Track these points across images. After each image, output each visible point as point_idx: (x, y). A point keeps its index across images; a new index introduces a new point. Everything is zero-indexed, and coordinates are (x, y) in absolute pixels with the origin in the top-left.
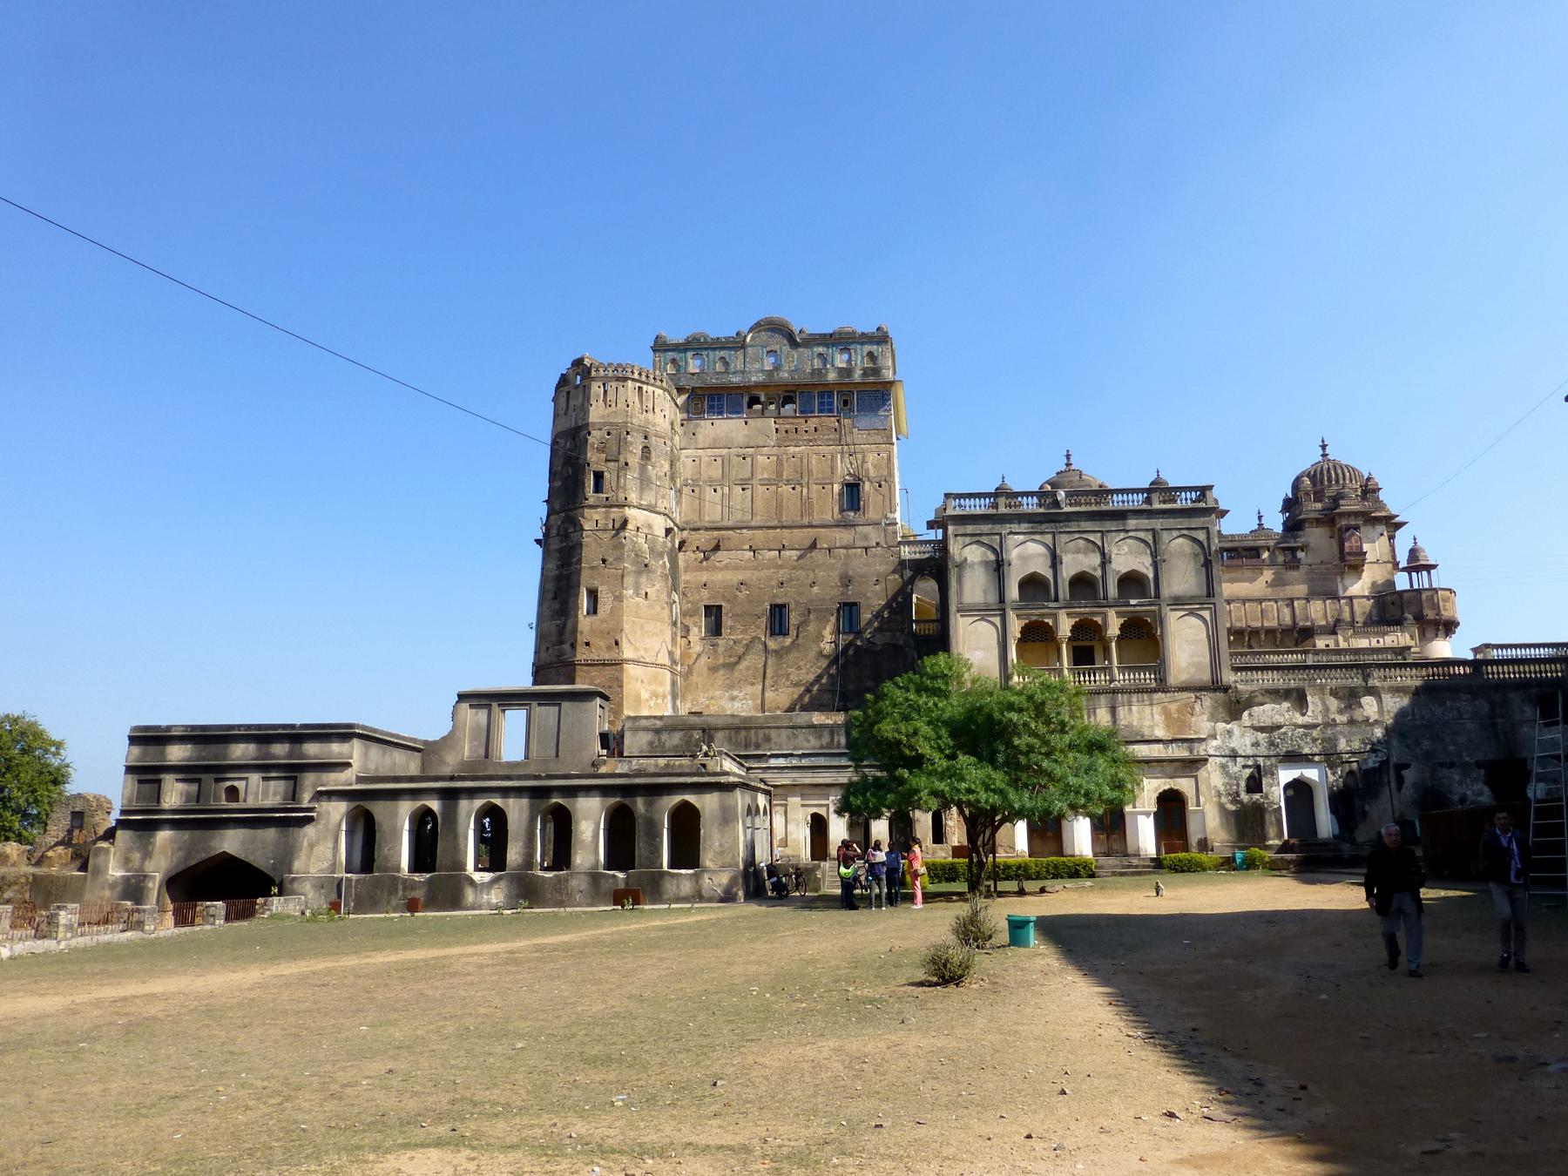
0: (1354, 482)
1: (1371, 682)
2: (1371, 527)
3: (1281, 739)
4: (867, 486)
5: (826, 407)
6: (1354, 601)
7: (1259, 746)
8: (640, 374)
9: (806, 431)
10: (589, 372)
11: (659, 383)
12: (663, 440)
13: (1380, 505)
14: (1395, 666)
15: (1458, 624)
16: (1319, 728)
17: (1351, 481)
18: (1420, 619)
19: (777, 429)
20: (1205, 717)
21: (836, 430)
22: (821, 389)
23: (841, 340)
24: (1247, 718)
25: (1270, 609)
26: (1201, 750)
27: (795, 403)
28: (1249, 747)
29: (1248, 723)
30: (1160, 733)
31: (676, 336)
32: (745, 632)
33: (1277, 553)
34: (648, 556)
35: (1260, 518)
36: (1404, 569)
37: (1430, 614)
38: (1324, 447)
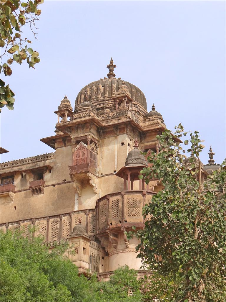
2: (114, 138)
6: (73, 215)
33: (28, 177)
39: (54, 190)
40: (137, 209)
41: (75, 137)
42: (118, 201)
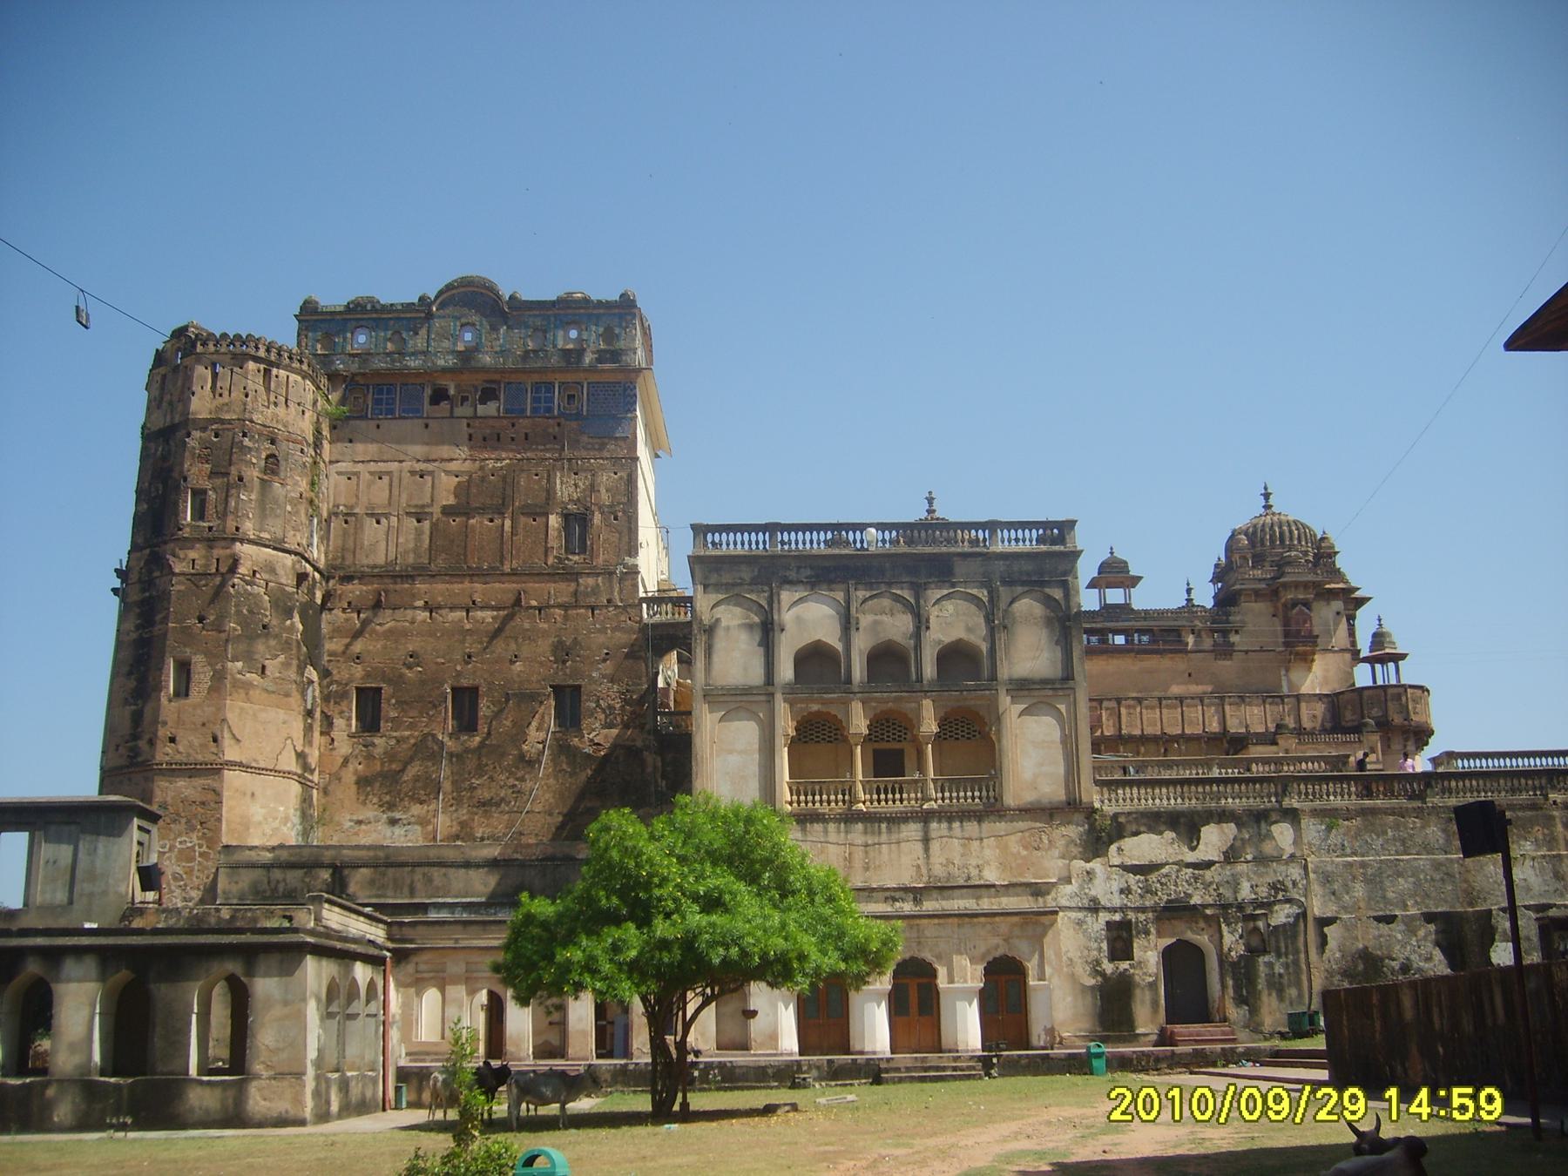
0: (1303, 543)
1: (1286, 803)
3: (1162, 884)
4: (597, 518)
5: (543, 405)
7: (1130, 893)
8: (268, 351)
9: (513, 439)
10: (194, 346)
11: (296, 365)
12: (299, 446)
13: (1337, 574)
14: (1327, 779)
15: (1432, 733)
16: (1213, 868)
17: (1299, 541)
18: (1384, 726)
19: (470, 435)
20: (1056, 853)
21: (555, 438)
22: (536, 378)
23: (569, 310)
24: (1115, 855)
26: (1050, 902)
27: (497, 398)
28: (1116, 895)
29: (1116, 861)
30: (992, 876)
31: (333, 298)
32: (412, 726)
34: (268, 613)
35: (1189, 591)
36: (1365, 660)
37: (1397, 720)
38: (1267, 496)
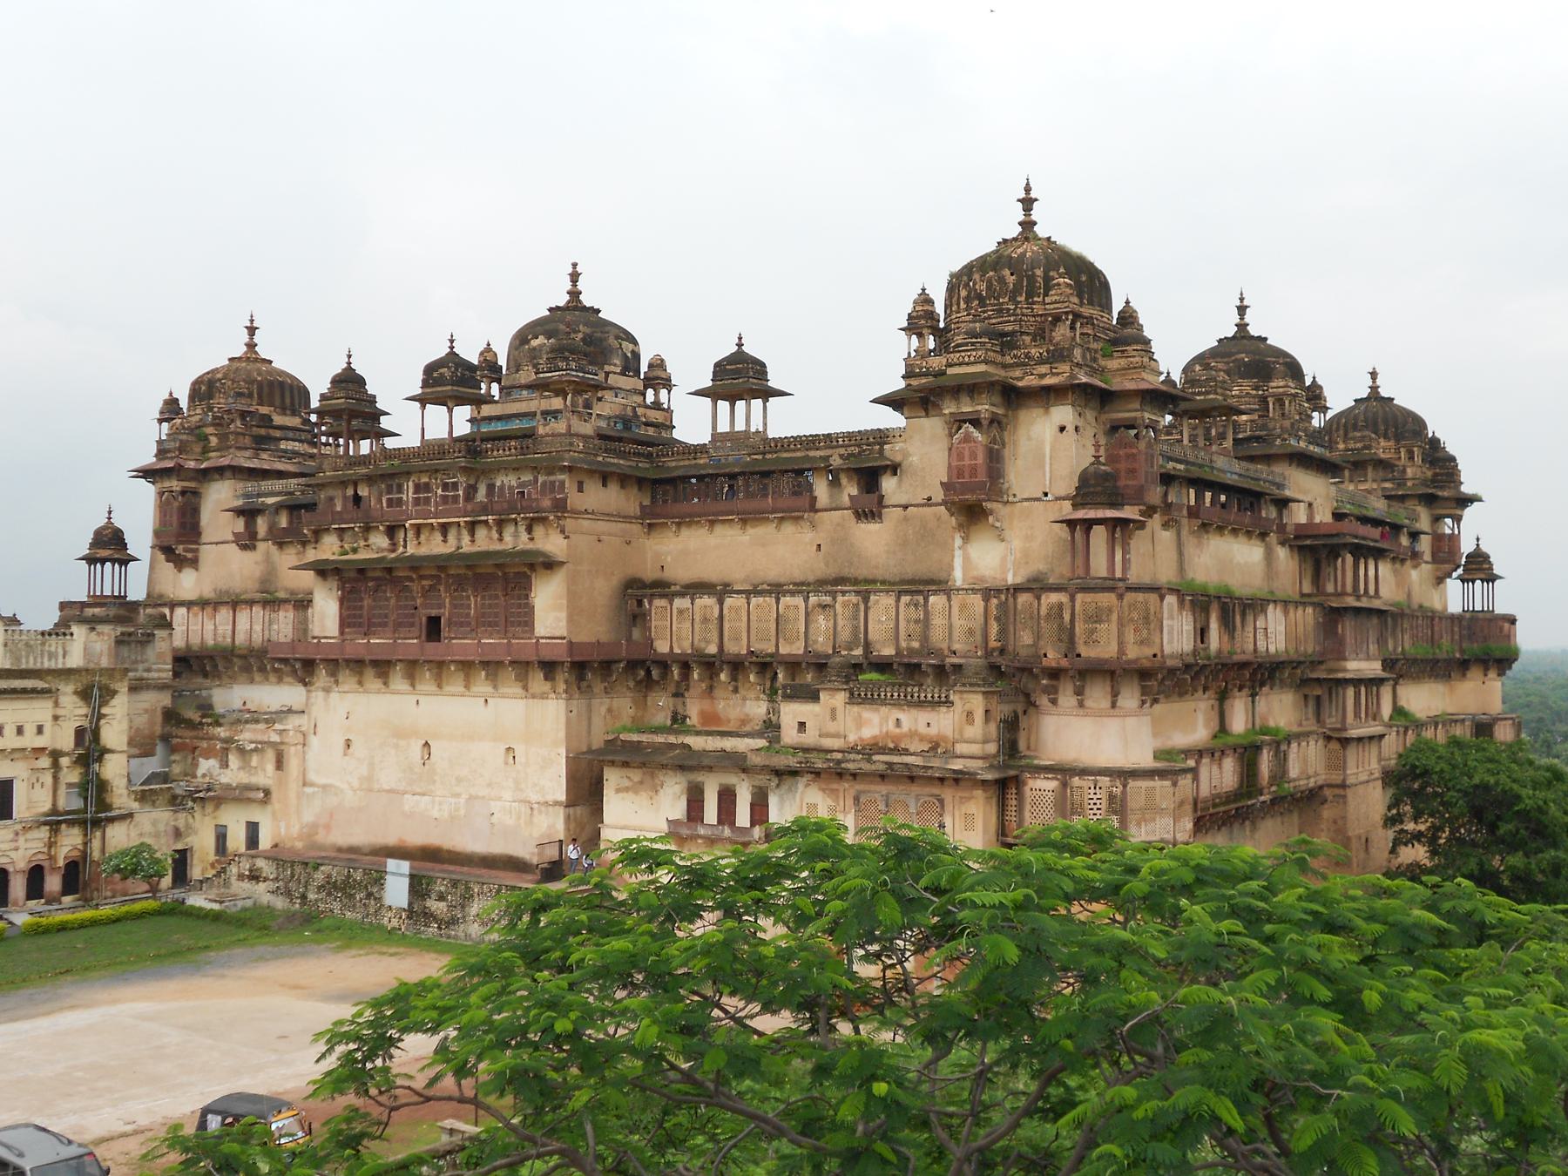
2: (1041, 411)
25: (791, 615)
33: (844, 480)
35: (1242, 310)
39: (906, 519)
40: (1104, 626)
41: (952, 410)
42: (1060, 606)
